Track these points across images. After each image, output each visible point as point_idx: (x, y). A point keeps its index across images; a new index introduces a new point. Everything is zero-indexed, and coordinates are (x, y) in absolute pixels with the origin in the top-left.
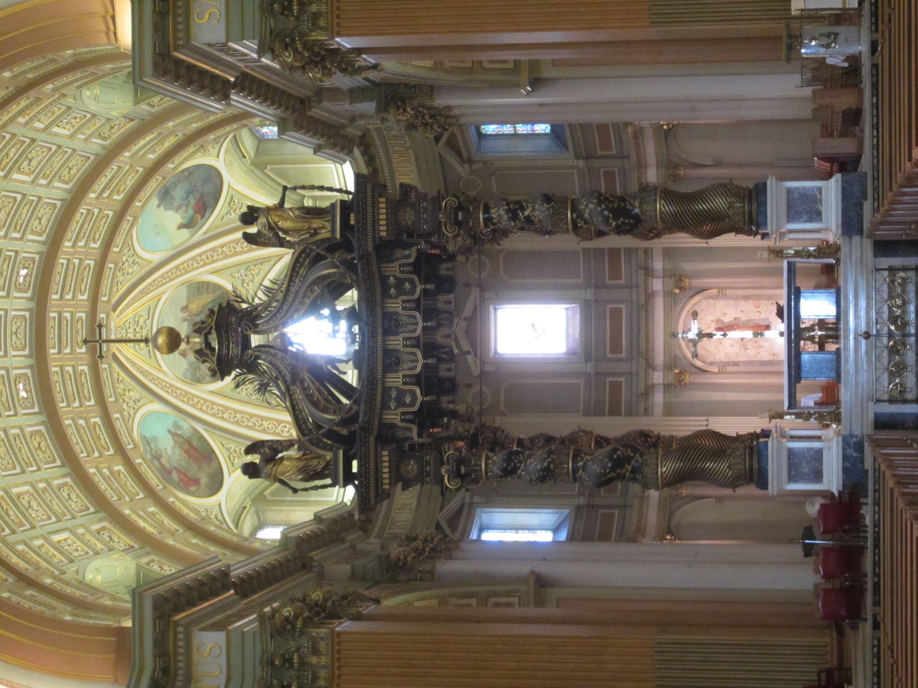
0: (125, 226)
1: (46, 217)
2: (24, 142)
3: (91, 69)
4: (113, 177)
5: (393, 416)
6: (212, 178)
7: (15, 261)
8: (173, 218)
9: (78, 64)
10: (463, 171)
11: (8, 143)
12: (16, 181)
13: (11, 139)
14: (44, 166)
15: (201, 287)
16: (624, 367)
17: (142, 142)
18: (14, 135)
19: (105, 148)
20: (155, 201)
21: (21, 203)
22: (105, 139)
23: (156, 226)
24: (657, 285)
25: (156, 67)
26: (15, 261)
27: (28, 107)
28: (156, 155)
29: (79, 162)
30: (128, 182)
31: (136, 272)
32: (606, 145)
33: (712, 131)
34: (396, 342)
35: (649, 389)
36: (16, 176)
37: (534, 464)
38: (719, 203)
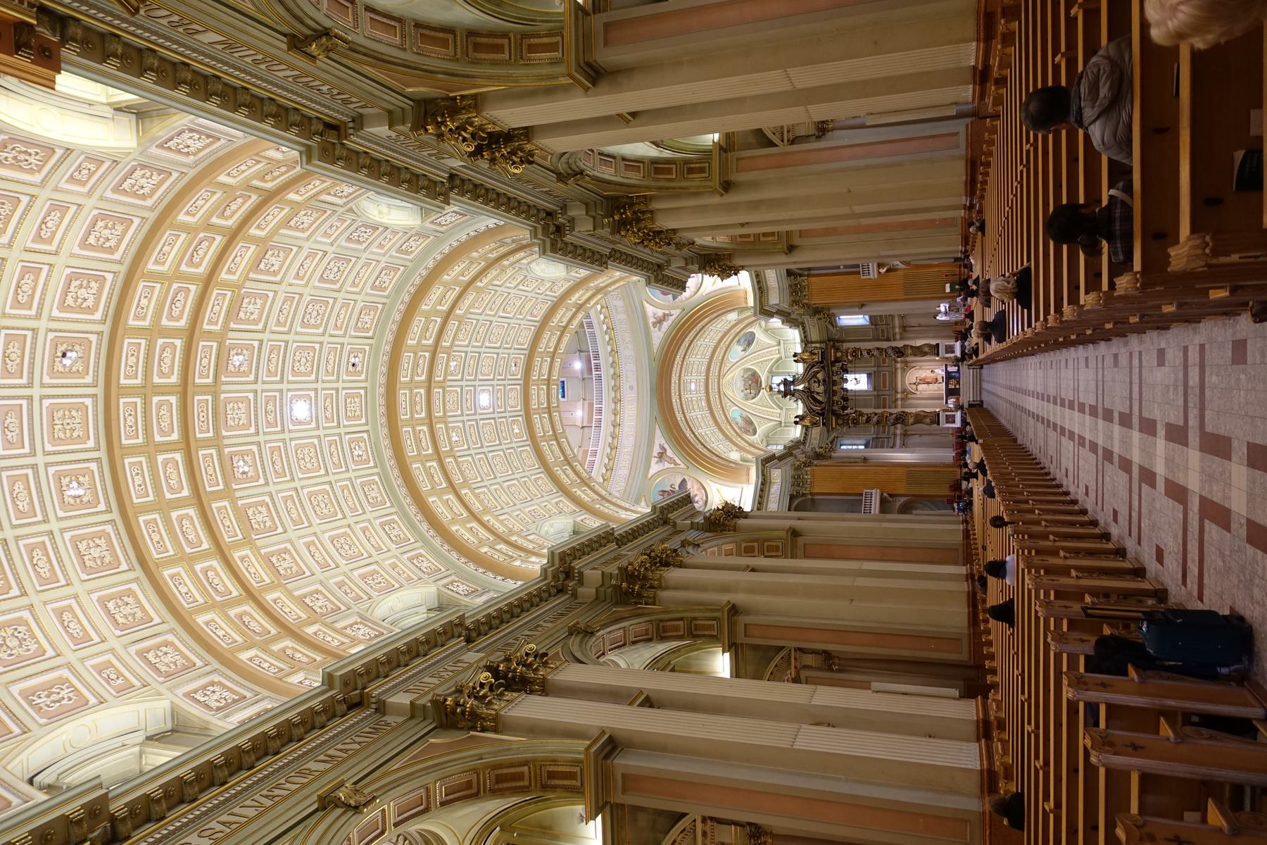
1: (710, 350)
5: (836, 408)
6: (753, 334)
8: (740, 348)
10: (834, 331)
15: (747, 370)
16: (887, 393)
24: (899, 365)
31: (729, 366)
32: (882, 321)
33: (918, 315)
34: (835, 388)
35: (896, 400)
37: (875, 419)
38: (926, 349)
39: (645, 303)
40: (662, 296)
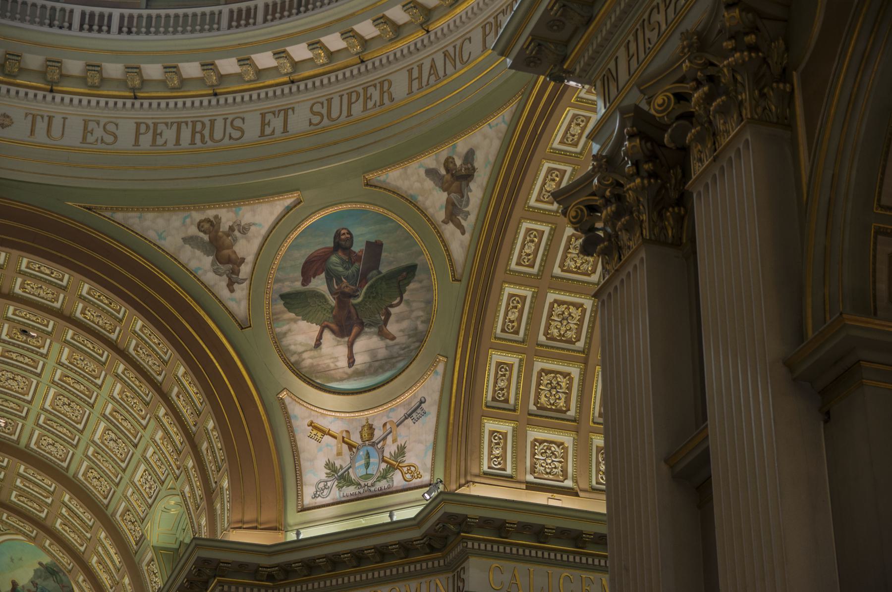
0: (27, 528)
1: (55, 452)
2: (135, 438)
3: (204, 504)
4: (82, 520)
7: (15, 415)
9: (210, 493)
11: (138, 422)
12: (97, 425)
13: (141, 425)
14: (107, 453)
17: (112, 551)
18: (145, 428)
19: (114, 514)
20: (46, 560)
21: (74, 427)
22: (122, 515)
23: (21, 559)
25: (206, 561)
26: (15, 415)
27: (173, 442)
28: (95, 565)
29: (103, 488)
30: (72, 535)
36: (102, 425)
39: (289, 200)
40: (301, 257)
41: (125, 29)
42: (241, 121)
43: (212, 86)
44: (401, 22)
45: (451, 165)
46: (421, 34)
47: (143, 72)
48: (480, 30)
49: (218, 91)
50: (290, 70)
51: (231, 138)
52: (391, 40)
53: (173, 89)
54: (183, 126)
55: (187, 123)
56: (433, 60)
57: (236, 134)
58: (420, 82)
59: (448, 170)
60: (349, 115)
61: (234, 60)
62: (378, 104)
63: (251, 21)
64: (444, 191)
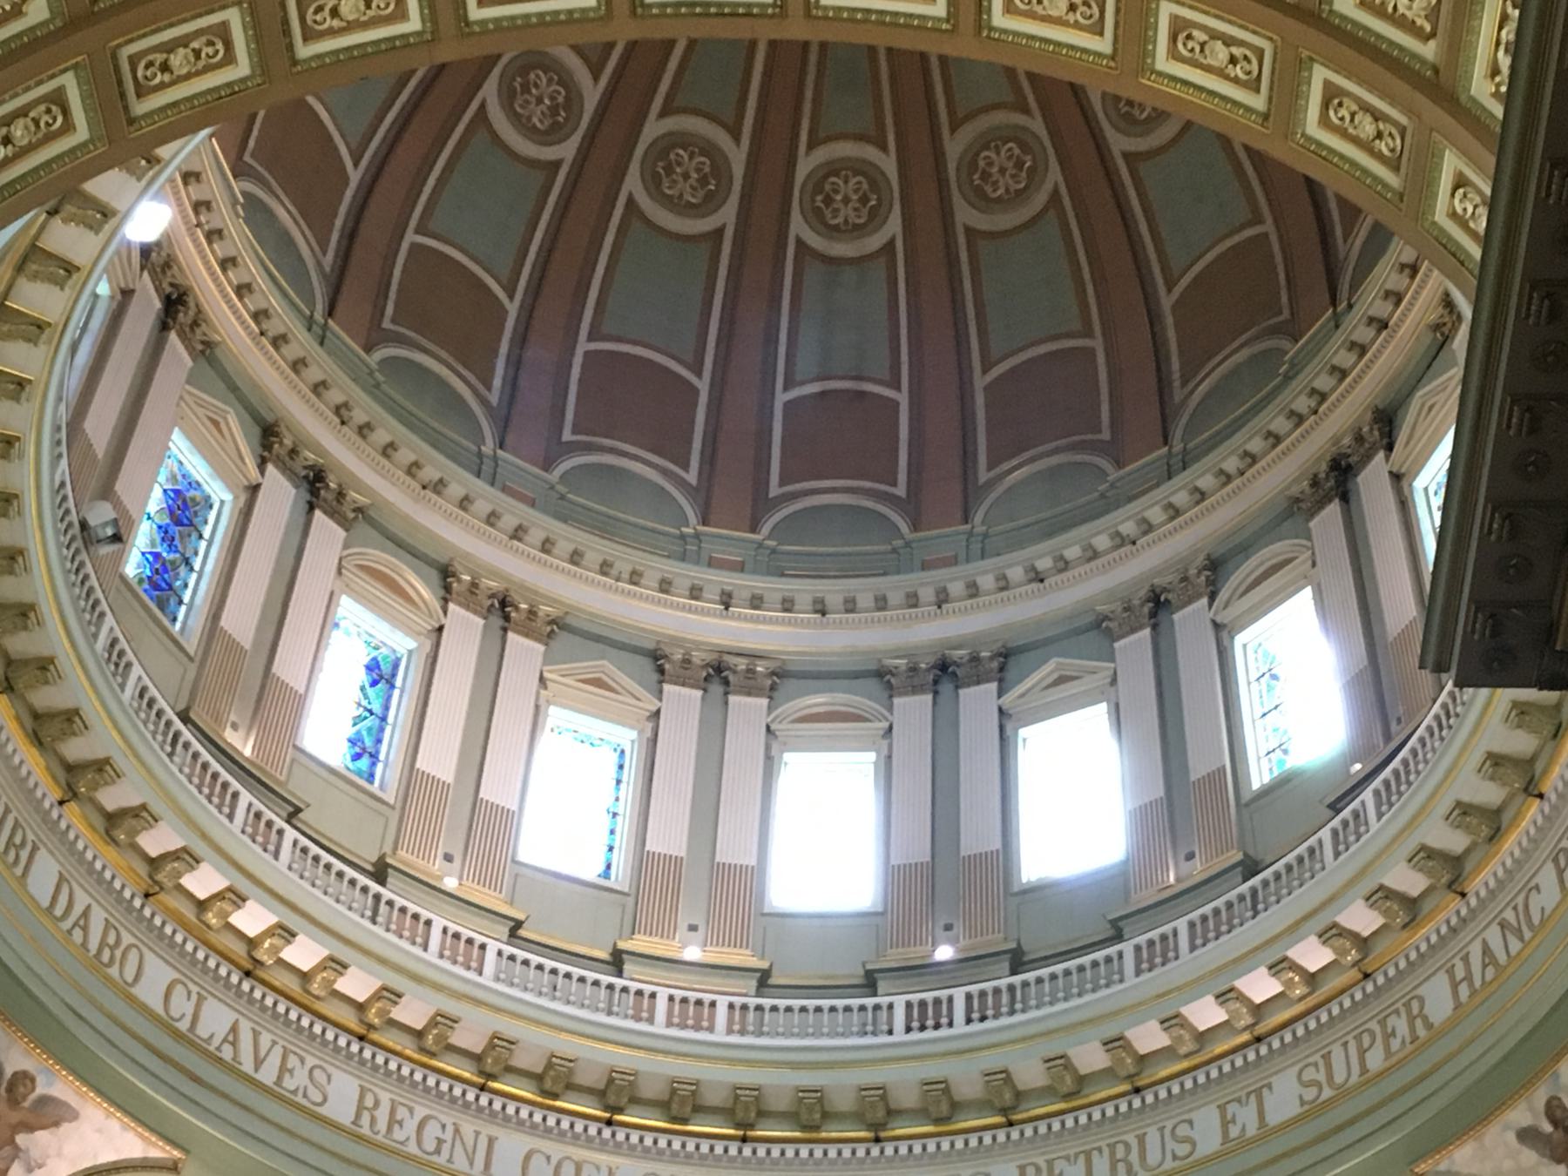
41: (975, 1016)
42: (1186, 1125)
43: (1130, 1077)
44: (1415, 893)
45: (1559, 1113)
46: (1456, 903)
47: (1014, 1077)
48: (1550, 866)
49: (1140, 1084)
50: (1248, 1020)
51: (1175, 1157)
52: (1405, 926)
53: (1068, 1096)
54: (1095, 1154)
55: (1100, 1150)
56: (1485, 942)
57: (1183, 1149)
58: (1471, 984)
59: (1555, 1122)
60: (1364, 1070)
61: (1154, 1025)
62: (1408, 1040)
63: (1171, 954)
64: (1559, 1162)
